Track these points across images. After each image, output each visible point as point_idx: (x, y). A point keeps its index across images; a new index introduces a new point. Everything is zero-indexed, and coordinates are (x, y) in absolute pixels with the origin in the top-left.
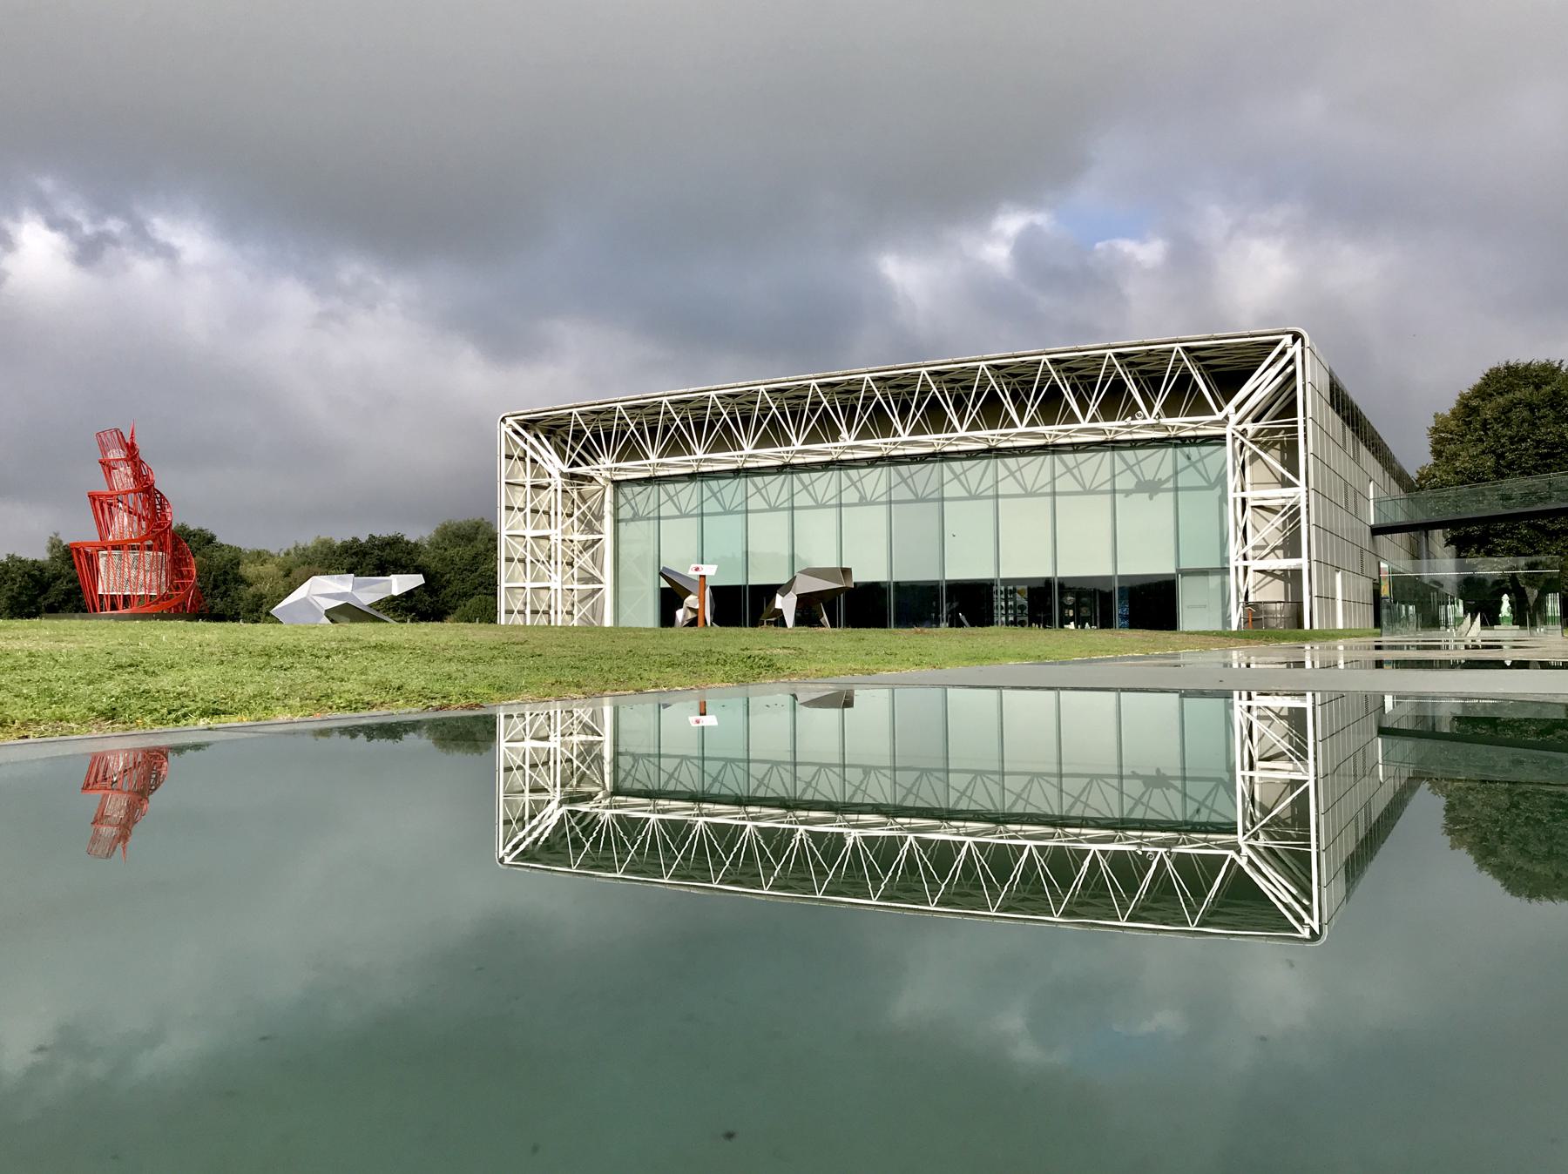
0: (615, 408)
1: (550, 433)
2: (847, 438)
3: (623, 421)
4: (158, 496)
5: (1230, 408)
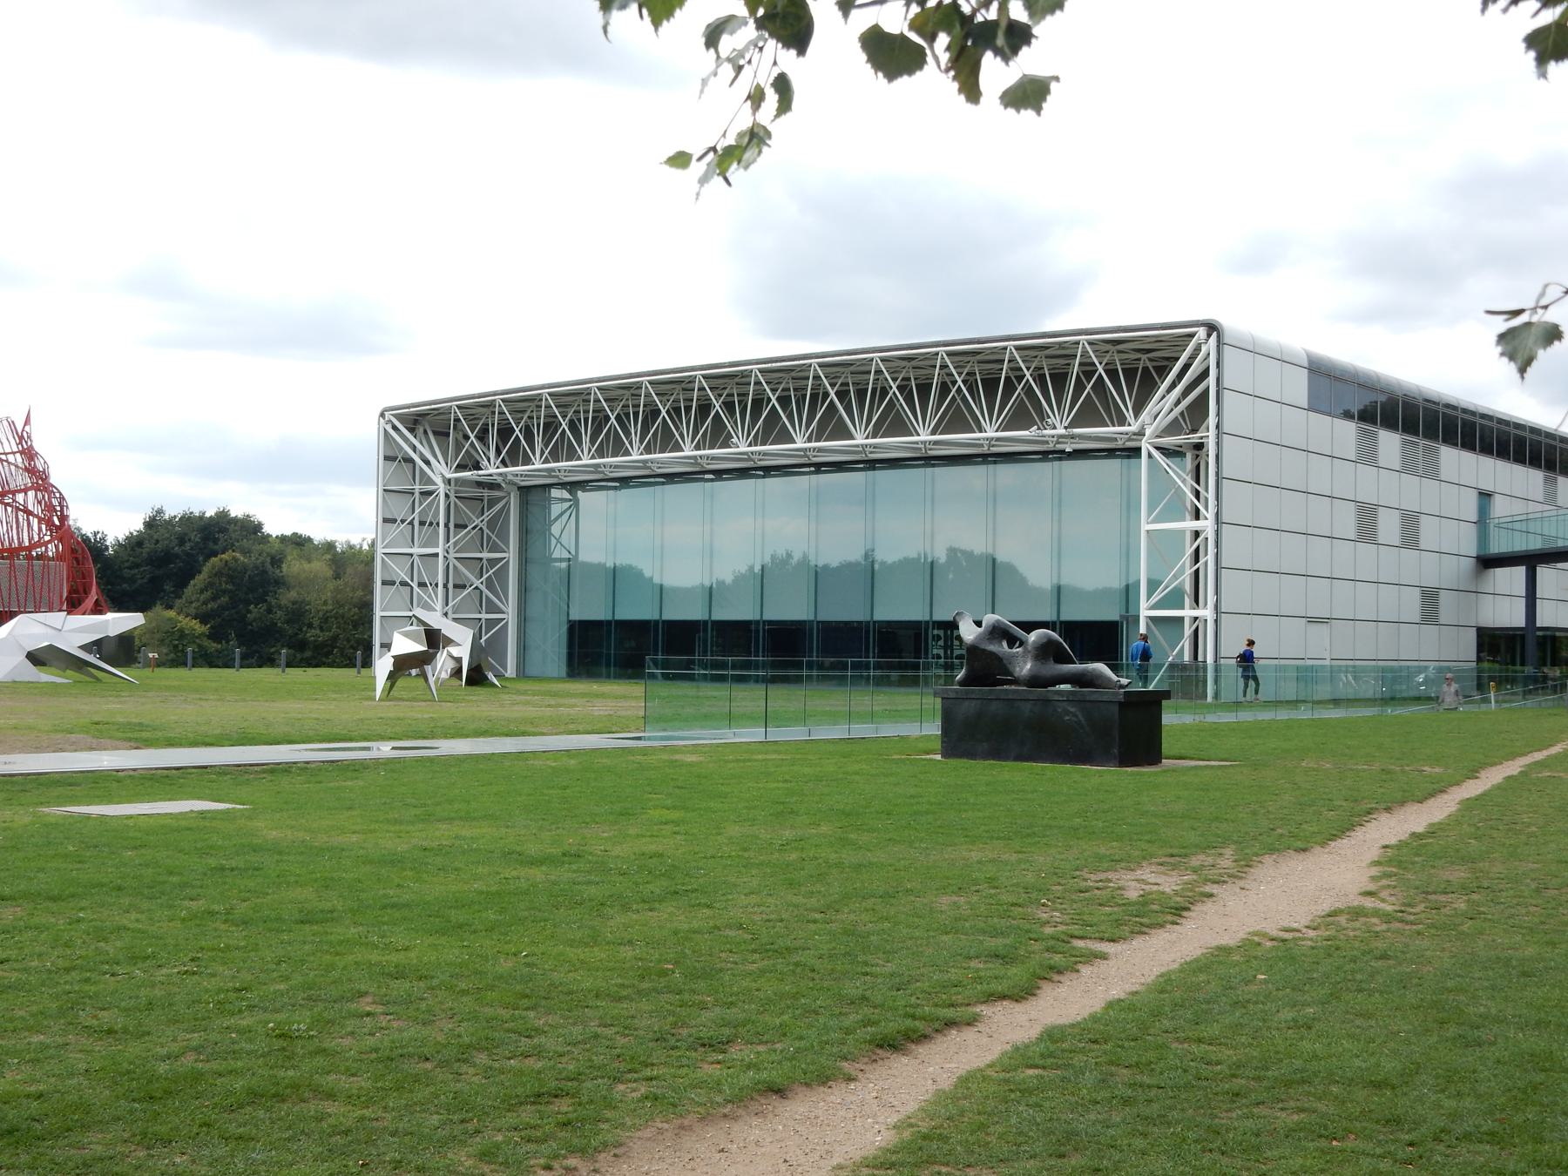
0: (811, 366)
1: (442, 434)
2: (741, 447)
3: (946, 370)
4: (58, 495)
5: (1145, 415)
